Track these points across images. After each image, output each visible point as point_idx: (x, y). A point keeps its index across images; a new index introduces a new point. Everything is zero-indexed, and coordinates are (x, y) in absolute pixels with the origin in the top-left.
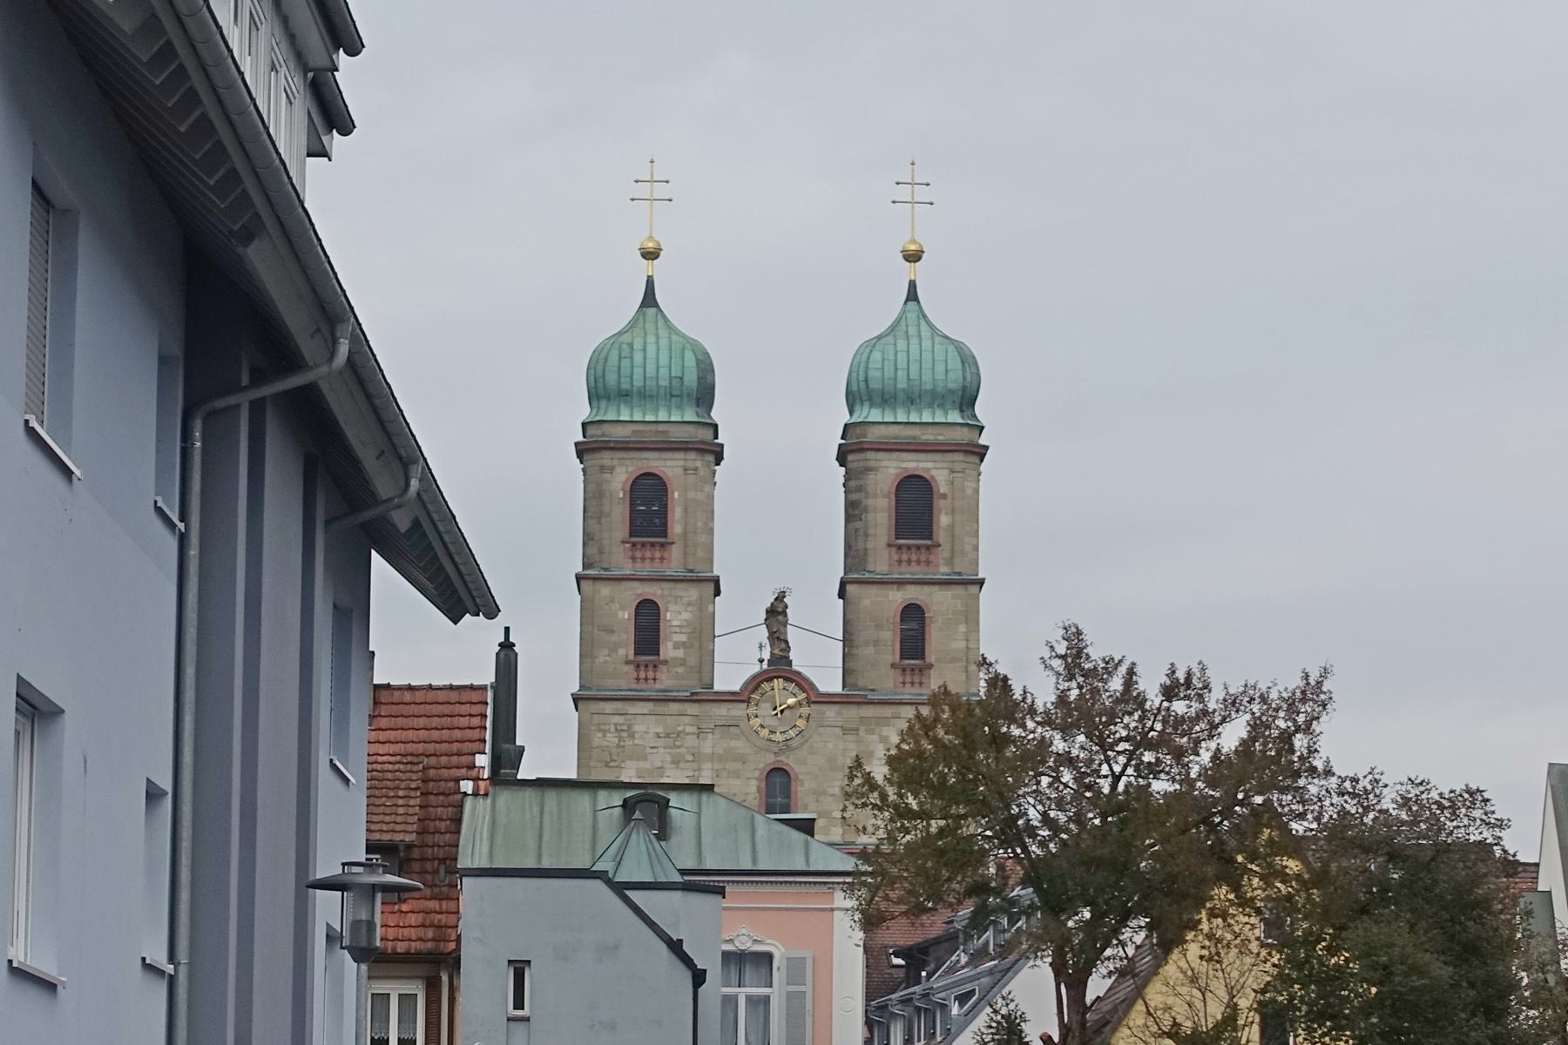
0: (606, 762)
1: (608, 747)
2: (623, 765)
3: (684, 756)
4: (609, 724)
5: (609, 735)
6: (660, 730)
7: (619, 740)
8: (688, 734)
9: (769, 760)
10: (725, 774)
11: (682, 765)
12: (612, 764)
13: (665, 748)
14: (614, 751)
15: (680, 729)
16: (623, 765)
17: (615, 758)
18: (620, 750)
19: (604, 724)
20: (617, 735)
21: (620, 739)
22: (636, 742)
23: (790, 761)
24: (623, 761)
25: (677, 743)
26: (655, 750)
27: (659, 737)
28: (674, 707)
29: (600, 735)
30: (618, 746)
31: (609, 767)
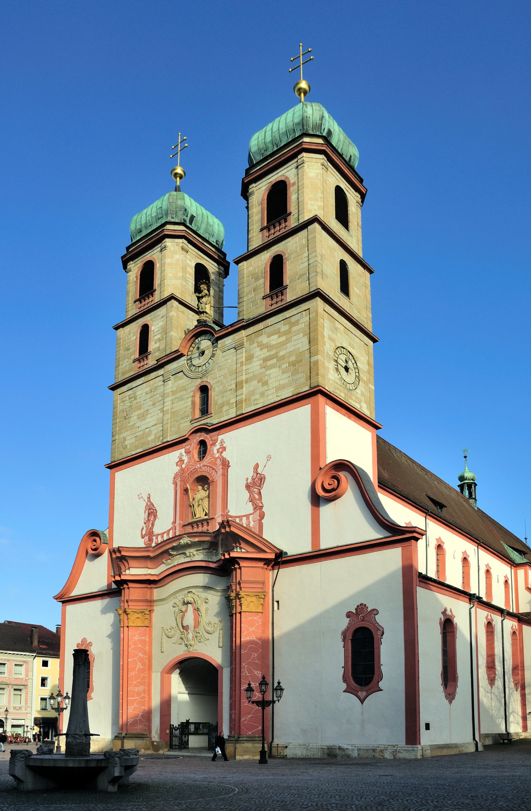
0: (125, 417)
2: (132, 416)
4: (126, 397)
9: (198, 383)
10: (176, 400)
11: (157, 404)
13: (150, 398)
15: (156, 385)
18: (130, 408)
19: (124, 398)
23: (210, 380)
25: (155, 393)
26: (145, 402)
28: (153, 375)
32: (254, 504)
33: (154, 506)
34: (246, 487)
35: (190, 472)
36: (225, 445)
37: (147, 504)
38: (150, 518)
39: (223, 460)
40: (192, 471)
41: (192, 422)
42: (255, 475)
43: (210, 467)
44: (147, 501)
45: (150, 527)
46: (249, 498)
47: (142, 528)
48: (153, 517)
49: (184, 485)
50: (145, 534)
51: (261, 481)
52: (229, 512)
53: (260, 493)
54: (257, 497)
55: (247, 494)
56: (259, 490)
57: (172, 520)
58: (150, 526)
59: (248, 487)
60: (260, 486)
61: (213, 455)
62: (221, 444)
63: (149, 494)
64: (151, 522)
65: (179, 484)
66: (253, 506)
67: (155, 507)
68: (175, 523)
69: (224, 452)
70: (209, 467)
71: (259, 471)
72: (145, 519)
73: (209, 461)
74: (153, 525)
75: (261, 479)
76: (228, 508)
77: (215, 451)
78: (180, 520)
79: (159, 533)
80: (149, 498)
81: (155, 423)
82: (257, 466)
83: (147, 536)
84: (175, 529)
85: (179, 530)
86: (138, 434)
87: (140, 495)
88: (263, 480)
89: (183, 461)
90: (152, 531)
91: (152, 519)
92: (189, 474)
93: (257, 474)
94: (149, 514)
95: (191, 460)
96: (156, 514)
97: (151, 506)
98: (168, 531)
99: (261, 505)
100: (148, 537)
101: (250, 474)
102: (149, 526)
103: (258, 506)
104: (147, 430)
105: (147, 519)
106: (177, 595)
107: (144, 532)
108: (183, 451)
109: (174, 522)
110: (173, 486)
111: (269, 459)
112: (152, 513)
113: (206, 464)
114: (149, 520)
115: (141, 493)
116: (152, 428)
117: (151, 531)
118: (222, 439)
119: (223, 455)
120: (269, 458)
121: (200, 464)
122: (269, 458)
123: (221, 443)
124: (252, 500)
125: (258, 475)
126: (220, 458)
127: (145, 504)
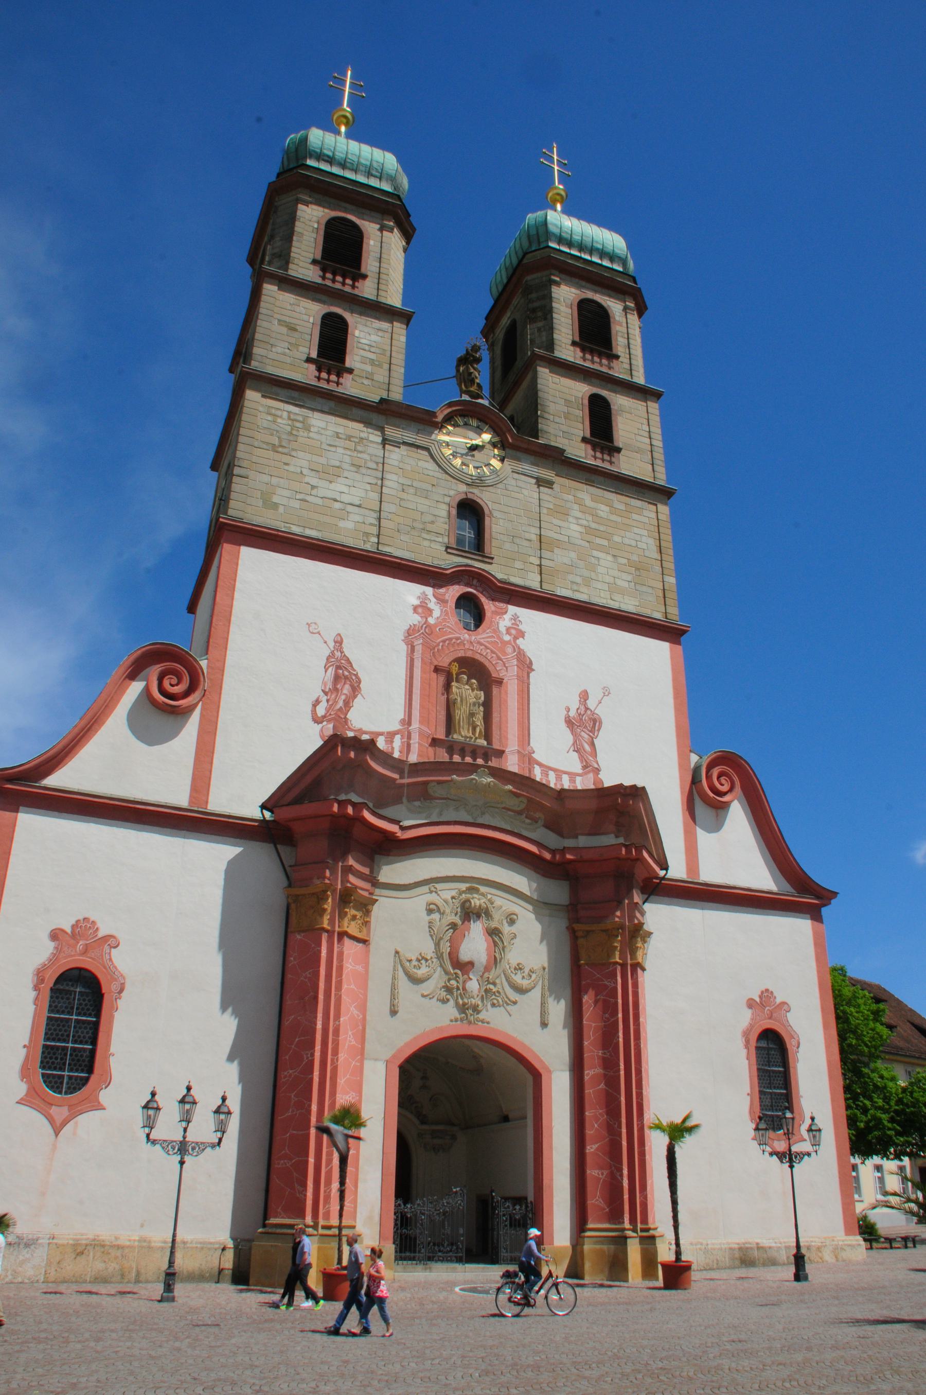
1: (277, 431)
2: (294, 453)
3: (365, 463)
5: (279, 420)
6: (340, 430)
7: (292, 429)
8: (372, 442)
12: (280, 449)
13: (345, 448)
14: (284, 436)
16: (294, 453)
17: (284, 444)
18: (291, 438)
20: (290, 422)
21: (293, 427)
22: (311, 435)
24: (293, 450)
26: (333, 449)
27: (338, 437)
29: (270, 418)
30: (291, 434)
31: (277, 452)
32: (582, 758)
33: (352, 666)
34: (566, 721)
35: (447, 640)
36: (521, 627)
37: (333, 652)
38: (339, 686)
39: (519, 653)
40: (451, 639)
41: (449, 550)
42: (582, 708)
43: (492, 652)
44: (334, 648)
45: (338, 707)
46: (573, 744)
47: (315, 699)
48: (347, 687)
49: (434, 659)
50: (324, 717)
51: (594, 724)
52: (534, 752)
53: (592, 745)
54: (587, 748)
55: (570, 738)
56: (592, 738)
57: (401, 716)
58: (341, 704)
59: (569, 722)
60: (592, 731)
61: (496, 631)
62: (513, 622)
63: (339, 635)
64: (343, 697)
65: (419, 649)
66: (582, 762)
67: (355, 671)
68: (409, 724)
69: (521, 639)
70: (488, 651)
71: (591, 704)
72: (325, 684)
73: (489, 640)
74: (348, 704)
75: (595, 721)
76: (531, 745)
77: (503, 629)
78: (421, 722)
79: (364, 729)
80: (339, 642)
81: (358, 503)
82: (584, 696)
83: (329, 721)
84: (409, 737)
85: (419, 744)
86: (308, 498)
87: (313, 626)
88: (597, 724)
89: (430, 612)
90: (345, 718)
91: (345, 691)
92: (444, 641)
93: (587, 709)
94: (337, 678)
95: (449, 618)
96: (358, 686)
97: (343, 661)
98: (388, 733)
99: (596, 766)
100: (331, 726)
101: (574, 704)
102: (336, 702)
103: (590, 766)
104: (337, 505)
105: (330, 685)
106: (436, 885)
107: (321, 711)
108: (429, 590)
109: (407, 721)
110: (403, 648)
111: (607, 694)
112: (346, 678)
113: (482, 640)
114: (335, 689)
115: (315, 623)
116: (350, 508)
117: (343, 717)
118: (516, 614)
119: (518, 641)
120: (606, 692)
121: (469, 635)
122: (606, 692)
123: (515, 620)
124: (578, 750)
125: (589, 712)
126: (513, 647)
127: (328, 652)
